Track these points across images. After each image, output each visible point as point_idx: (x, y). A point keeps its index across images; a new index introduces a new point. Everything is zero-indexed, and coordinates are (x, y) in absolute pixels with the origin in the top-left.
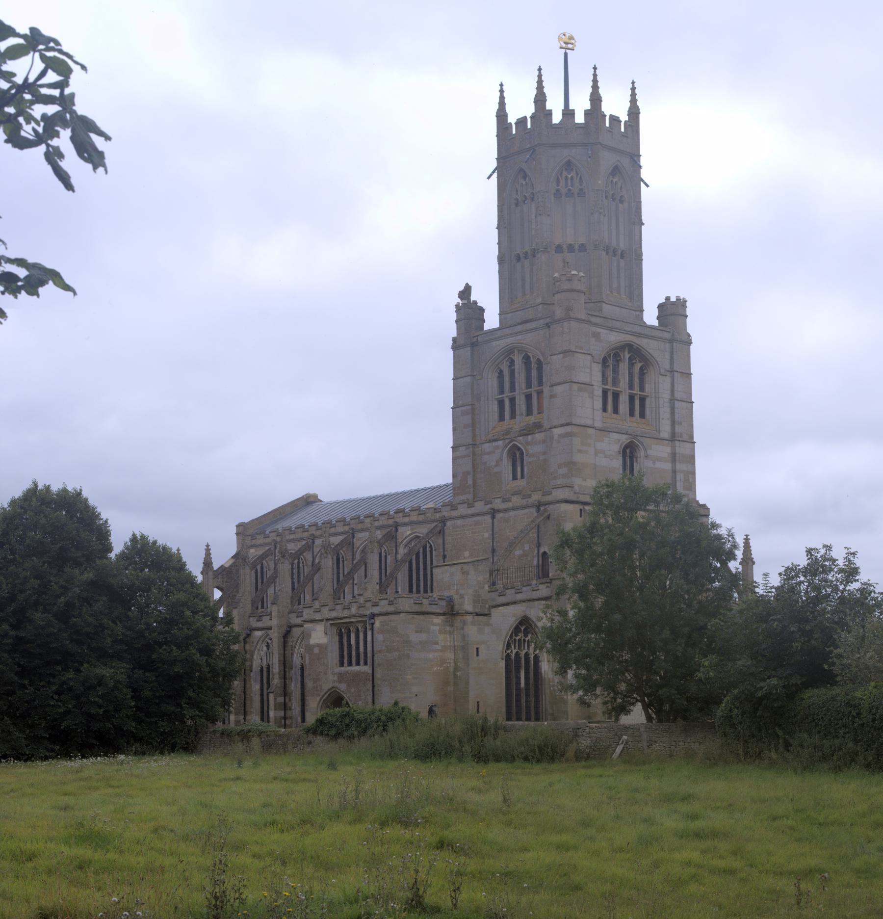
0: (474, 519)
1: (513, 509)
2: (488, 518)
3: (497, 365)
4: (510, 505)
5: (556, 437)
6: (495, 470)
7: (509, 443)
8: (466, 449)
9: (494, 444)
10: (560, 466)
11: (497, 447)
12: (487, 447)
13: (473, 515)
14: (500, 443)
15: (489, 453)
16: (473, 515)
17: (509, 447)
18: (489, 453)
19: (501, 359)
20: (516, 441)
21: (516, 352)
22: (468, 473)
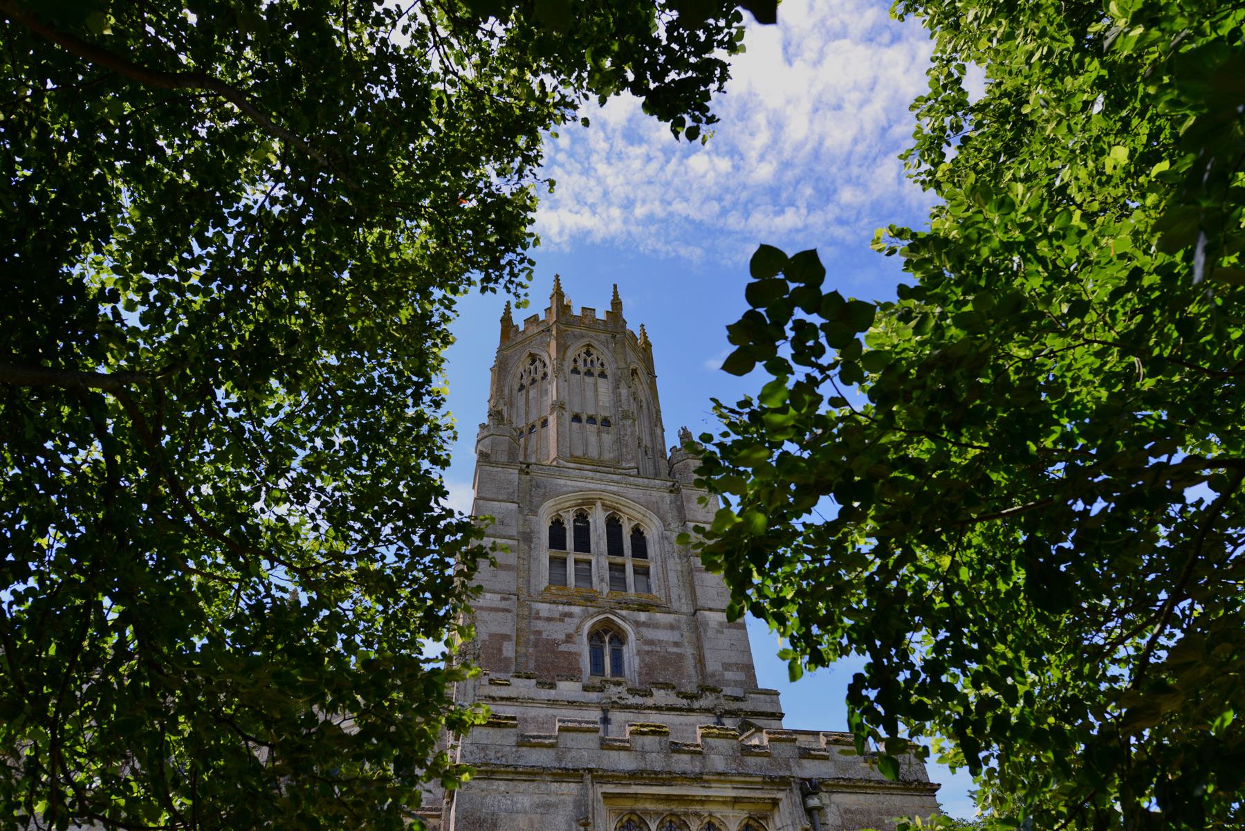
0: (551, 712)
1: (658, 708)
2: (595, 715)
4: (650, 701)
6: (563, 648)
7: (599, 613)
8: (503, 599)
9: (567, 609)
10: (727, 667)
11: (570, 615)
12: (544, 609)
13: (553, 703)
14: (576, 610)
15: (549, 619)
16: (553, 703)
17: (595, 619)
18: (549, 619)
19: (568, 504)
21: (599, 503)
22: (506, 637)
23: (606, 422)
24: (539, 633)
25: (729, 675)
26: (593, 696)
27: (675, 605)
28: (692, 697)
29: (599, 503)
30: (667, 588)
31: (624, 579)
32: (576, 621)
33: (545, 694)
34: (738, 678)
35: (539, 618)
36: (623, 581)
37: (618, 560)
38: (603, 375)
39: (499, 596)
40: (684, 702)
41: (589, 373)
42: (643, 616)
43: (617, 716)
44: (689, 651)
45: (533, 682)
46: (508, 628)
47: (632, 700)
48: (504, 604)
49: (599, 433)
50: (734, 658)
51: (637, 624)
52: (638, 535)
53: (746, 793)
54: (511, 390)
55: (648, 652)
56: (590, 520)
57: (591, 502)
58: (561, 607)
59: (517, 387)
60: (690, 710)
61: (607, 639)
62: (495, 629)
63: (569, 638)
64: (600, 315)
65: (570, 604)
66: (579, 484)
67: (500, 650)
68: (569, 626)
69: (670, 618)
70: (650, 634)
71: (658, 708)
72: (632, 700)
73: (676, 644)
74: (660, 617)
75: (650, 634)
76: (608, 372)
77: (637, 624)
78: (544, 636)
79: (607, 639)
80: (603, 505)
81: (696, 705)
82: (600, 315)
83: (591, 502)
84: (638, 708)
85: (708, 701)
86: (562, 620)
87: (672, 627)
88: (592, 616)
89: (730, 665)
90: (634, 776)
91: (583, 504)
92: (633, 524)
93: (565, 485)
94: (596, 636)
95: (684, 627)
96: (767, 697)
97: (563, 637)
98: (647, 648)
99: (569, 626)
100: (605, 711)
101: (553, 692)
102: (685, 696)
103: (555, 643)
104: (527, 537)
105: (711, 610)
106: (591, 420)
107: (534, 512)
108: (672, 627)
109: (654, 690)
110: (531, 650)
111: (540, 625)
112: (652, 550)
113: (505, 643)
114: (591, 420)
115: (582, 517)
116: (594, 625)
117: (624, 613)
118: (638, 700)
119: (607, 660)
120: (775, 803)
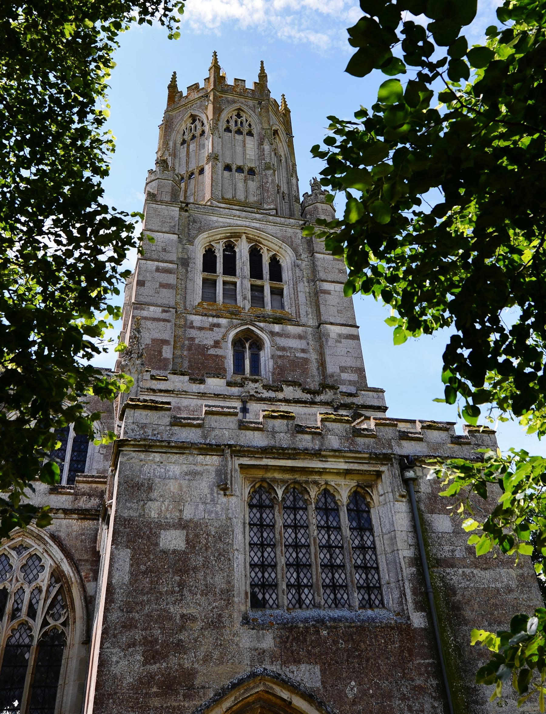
1: (286, 401)
3: (210, 242)
4: (281, 396)
5: (333, 335)
6: (212, 352)
7: (242, 325)
8: (164, 311)
9: (215, 320)
10: (343, 369)
11: (218, 325)
12: (197, 320)
13: (202, 395)
14: (223, 321)
15: (201, 329)
16: (202, 395)
17: (238, 330)
18: (201, 329)
19: (218, 237)
20: (254, 325)
21: (244, 237)
22: (165, 342)
23: (252, 172)
24: (192, 339)
25: (345, 376)
26: (235, 390)
27: (303, 320)
28: (315, 393)
29: (244, 237)
30: (297, 306)
31: (263, 298)
32: (223, 330)
33: (196, 388)
34: (352, 379)
35: (193, 327)
36: (262, 299)
37: (259, 282)
38: (250, 134)
39: (160, 309)
40: (309, 396)
41: (239, 132)
42: (277, 328)
43: (253, 406)
44: (313, 356)
45: (187, 378)
46: (167, 335)
47: (266, 394)
48: (165, 316)
49: (245, 181)
50: (349, 362)
51: (272, 334)
52: (275, 264)
53: (356, 467)
54: (175, 144)
55: (280, 357)
56: (237, 250)
57: (237, 236)
58: (211, 319)
59: (179, 141)
60: (313, 403)
61: (247, 345)
62: (157, 335)
63: (217, 344)
64: (250, 85)
65: (218, 317)
66: (228, 220)
67: (160, 352)
68: (217, 334)
69: (298, 330)
70: (282, 342)
71: (286, 401)
72: (266, 394)
73: (303, 351)
74: (291, 329)
75: (282, 342)
76: (254, 132)
77: (272, 334)
78: (197, 341)
79: (247, 345)
80: (247, 238)
81: (318, 399)
82: (250, 85)
83: (237, 236)
84: (271, 400)
85: (327, 396)
86: (212, 330)
87: (300, 337)
88: (236, 327)
89: (346, 368)
90: (266, 451)
91: (231, 237)
92: (271, 254)
93: (217, 222)
94: (238, 343)
95: (310, 337)
96: (375, 394)
97: (212, 343)
98: (280, 353)
99: (217, 334)
100: (244, 402)
101: (202, 386)
102: (309, 392)
103: (205, 348)
104: (185, 262)
105: (332, 324)
106: (240, 169)
107: (191, 242)
108: (300, 337)
109: (284, 387)
110: (185, 353)
111: (193, 333)
112: (286, 275)
113: (165, 347)
114: (240, 169)
115: (230, 248)
116: (237, 333)
117: (262, 325)
118: (271, 394)
119: (247, 362)
120: (379, 474)
